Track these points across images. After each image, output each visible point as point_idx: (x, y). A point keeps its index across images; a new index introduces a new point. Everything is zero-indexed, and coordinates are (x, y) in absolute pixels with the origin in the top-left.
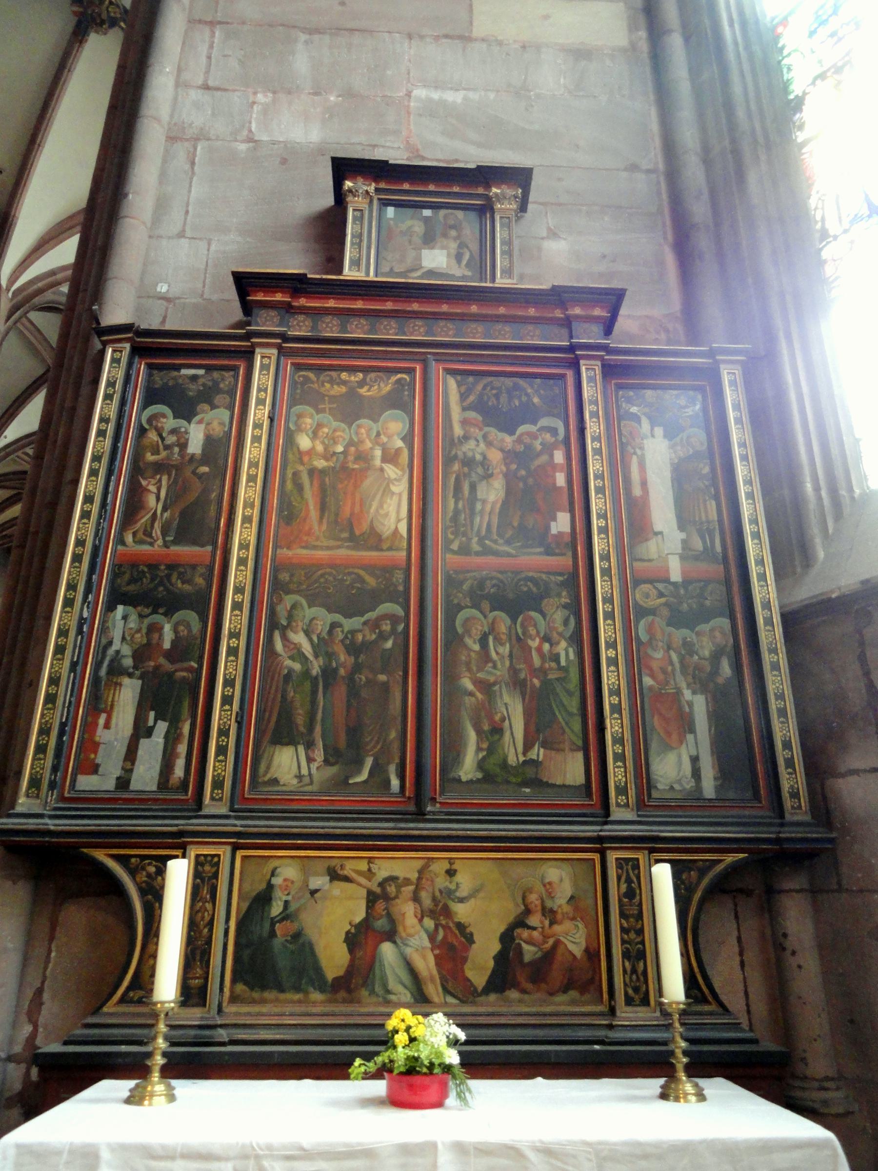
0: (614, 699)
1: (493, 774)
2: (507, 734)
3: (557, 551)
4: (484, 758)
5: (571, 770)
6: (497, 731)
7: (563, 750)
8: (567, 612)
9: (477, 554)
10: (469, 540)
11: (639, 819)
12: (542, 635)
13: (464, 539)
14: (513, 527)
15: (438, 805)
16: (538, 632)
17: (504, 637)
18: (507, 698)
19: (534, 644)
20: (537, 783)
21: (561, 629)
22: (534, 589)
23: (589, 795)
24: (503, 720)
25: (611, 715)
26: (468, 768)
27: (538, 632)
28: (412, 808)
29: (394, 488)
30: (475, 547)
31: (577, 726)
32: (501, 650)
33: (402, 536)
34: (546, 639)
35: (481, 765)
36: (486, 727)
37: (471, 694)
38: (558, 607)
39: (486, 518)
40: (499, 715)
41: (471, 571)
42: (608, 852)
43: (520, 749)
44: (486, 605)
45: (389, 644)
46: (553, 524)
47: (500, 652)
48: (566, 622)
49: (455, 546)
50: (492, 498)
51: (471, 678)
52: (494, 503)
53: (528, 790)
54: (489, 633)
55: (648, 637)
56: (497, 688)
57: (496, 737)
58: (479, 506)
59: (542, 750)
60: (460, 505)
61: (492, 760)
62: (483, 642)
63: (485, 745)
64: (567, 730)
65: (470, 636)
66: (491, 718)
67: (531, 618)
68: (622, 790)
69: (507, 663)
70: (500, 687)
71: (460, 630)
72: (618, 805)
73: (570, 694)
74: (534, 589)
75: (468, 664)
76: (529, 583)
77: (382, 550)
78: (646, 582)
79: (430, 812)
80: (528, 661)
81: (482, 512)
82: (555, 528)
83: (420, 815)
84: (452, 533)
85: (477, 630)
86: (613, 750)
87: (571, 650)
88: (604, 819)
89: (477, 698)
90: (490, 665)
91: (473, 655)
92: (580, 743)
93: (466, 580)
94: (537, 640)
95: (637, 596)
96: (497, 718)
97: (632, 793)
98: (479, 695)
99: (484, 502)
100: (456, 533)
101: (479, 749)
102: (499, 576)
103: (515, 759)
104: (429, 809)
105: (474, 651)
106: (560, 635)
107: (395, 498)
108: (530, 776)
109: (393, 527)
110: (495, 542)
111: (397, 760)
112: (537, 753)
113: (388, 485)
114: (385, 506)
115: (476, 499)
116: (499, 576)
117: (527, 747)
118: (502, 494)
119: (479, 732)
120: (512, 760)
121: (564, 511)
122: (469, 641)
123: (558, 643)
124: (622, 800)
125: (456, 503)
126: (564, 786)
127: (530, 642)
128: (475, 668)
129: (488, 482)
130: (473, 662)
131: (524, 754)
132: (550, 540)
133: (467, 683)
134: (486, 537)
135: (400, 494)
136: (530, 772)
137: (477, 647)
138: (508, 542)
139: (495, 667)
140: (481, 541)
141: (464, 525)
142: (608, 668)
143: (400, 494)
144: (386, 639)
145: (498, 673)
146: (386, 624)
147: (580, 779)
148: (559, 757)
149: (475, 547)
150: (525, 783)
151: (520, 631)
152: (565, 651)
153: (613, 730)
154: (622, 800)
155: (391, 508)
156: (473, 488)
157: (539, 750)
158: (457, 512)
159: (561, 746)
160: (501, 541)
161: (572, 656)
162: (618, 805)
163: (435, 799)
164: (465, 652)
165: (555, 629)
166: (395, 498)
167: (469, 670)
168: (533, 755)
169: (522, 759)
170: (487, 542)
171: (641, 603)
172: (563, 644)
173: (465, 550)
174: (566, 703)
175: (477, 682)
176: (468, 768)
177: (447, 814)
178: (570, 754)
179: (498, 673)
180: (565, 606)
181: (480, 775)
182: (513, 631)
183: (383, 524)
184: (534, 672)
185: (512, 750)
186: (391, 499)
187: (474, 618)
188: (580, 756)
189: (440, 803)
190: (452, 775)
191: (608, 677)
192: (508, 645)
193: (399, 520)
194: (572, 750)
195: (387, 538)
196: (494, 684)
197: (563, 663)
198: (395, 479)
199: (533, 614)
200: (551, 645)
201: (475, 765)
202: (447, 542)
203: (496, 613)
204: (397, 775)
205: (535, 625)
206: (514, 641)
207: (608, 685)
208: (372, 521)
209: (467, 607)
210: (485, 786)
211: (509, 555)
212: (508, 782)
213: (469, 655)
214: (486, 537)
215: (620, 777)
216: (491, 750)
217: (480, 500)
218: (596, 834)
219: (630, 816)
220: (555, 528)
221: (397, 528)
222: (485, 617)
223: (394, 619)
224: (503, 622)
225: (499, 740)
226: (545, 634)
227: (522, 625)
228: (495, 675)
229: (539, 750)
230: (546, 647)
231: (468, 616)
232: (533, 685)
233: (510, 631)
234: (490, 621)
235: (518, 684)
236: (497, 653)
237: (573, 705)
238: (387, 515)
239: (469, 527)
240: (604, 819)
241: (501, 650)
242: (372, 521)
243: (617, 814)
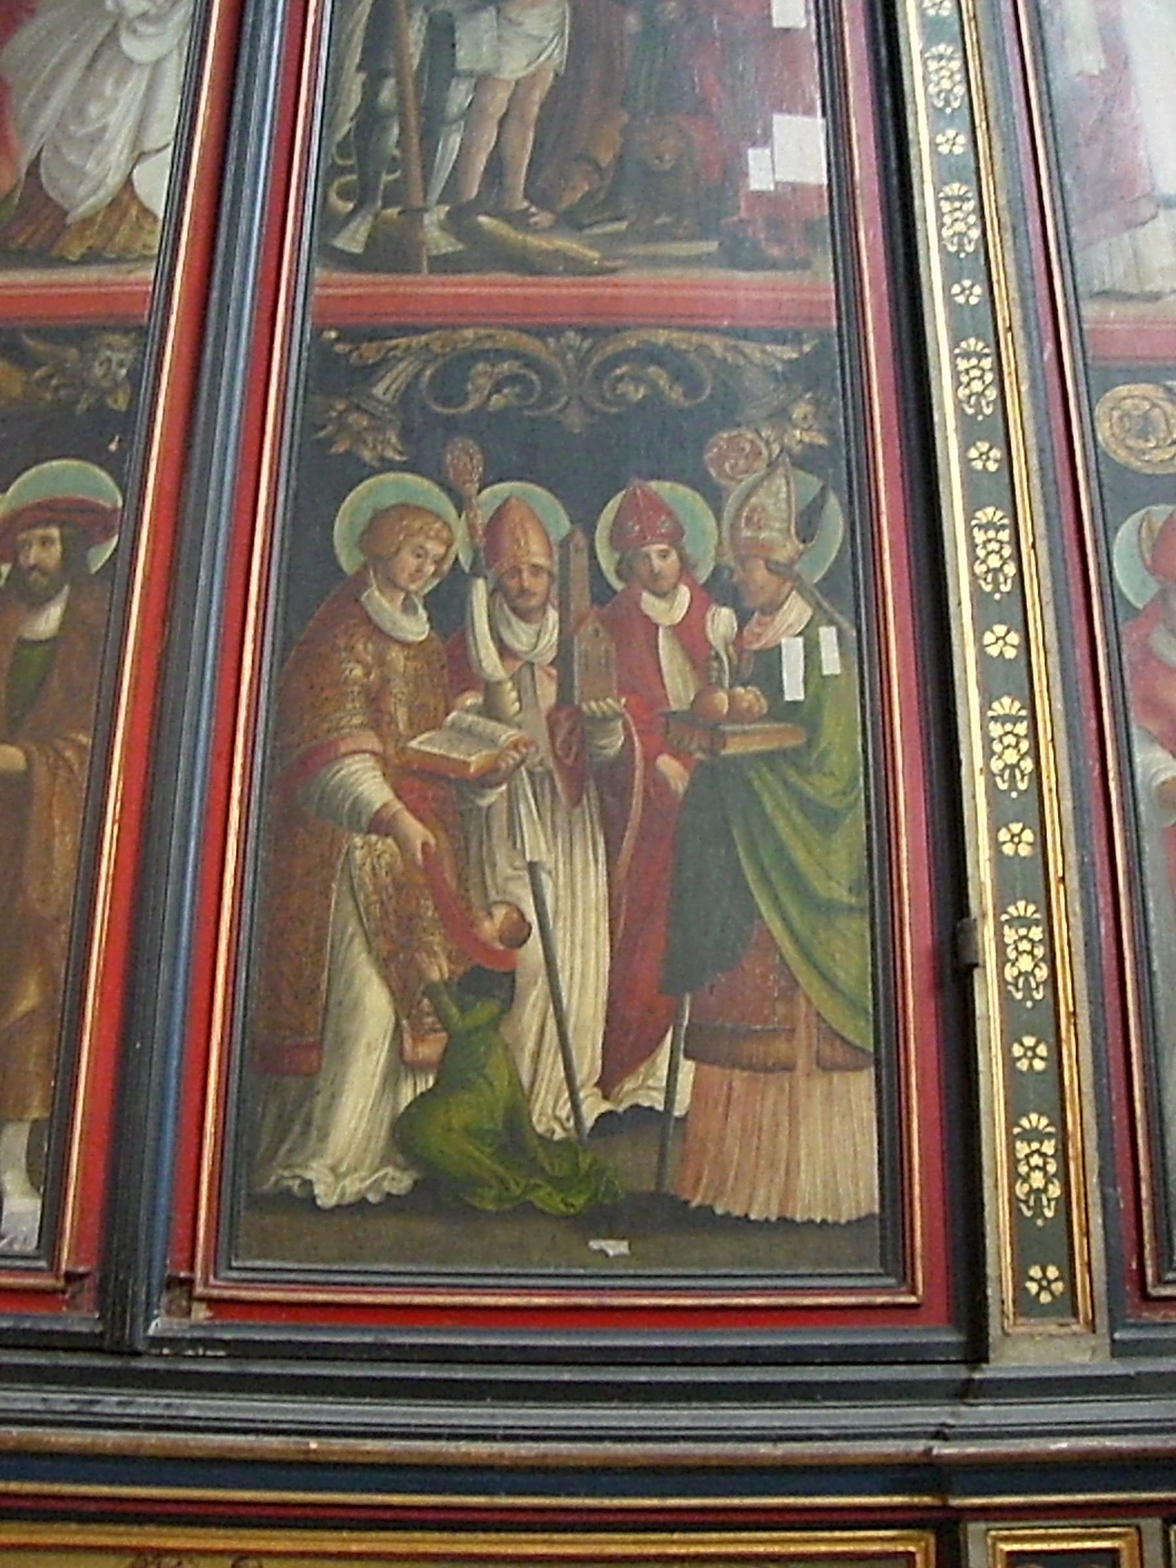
0: (1015, 838)
1: (462, 1166)
2: (534, 998)
3: (775, 252)
4: (420, 1101)
5: (823, 1151)
6: (489, 982)
7: (789, 1067)
8: (813, 484)
9: (444, 264)
10: (413, 215)
11: (1118, 1368)
12: (703, 575)
13: (392, 212)
14: (598, 168)
15: (201, 1313)
16: (686, 568)
17: (538, 585)
18: (536, 842)
19: (669, 610)
20: (664, 1215)
21: (787, 549)
22: (676, 395)
23: (898, 1264)
24: (517, 935)
25: (1000, 909)
26: (348, 1144)
27: (686, 568)
28: (81, 1320)
29: (129, 45)
30: (435, 234)
31: (851, 960)
32: (520, 636)
33: (146, 212)
34: (719, 589)
35: (404, 1135)
36: (438, 969)
37: (381, 825)
38: (772, 465)
39: (489, 138)
40: (500, 913)
41: (417, 331)
42: (975, 1528)
43: (589, 1062)
44: (464, 457)
45: (49, 621)
46: (756, 158)
47: (520, 646)
48: (808, 525)
49: (352, 240)
50: (515, 66)
51: (381, 758)
52: (521, 87)
53: (616, 1248)
54: (475, 573)
55: (1153, 588)
56: (493, 797)
57: (484, 1011)
58: (459, 96)
59: (687, 1068)
60: (387, 94)
61: (462, 1112)
62: (447, 606)
63: (430, 1050)
64: (804, 975)
65: (390, 584)
66: (459, 925)
67: (658, 506)
68: (1044, 1240)
69: (548, 693)
70: (512, 798)
71: (348, 559)
72: (1025, 1305)
73: (825, 820)
74: (676, 395)
75: (374, 700)
76: (652, 369)
77: (63, 262)
78: (1132, 377)
79: (158, 1342)
80: (642, 684)
81: (472, 115)
82: (762, 172)
83: (112, 1355)
84: (344, 194)
85: (419, 562)
86: (1010, 1062)
87: (827, 635)
88: (962, 1373)
89: (403, 843)
90: (471, 699)
91: (396, 656)
92: (861, 1033)
93: (384, 363)
94: (684, 594)
95: (1104, 432)
96: (490, 928)
97: (1091, 1247)
98: (416, 831)
99: (482, 81)
100: (362, 196)
101: (400, 1064)
102: (532, 345)
103: (565, 1110)
104: (154, 1328)
105: (405, 645)
106: (783, 572)
107: (137, 83)
108: (628, 1183)
109: (114, 180)
110: (519, 220)
111: (36, 1111)
112: (667, 1080)
113: (112, 36)
114: (93, 110)
115: (454, 74)
116: (532, 345)
117: (623, 1052)
118: (556, 54)
119: (405, 994)
120: (549, 1113)
121: (808, 111)
122: (382, 604)
123: (773, 607)
124: (1045, 1284)
125: (371, 91)
126: (785, 1223)
127: (650, 604)
128: (402, 715)
129: (499, 11)
130: (398, 687)
131: (606, 1085)
132: (743, 214)
133: (369, 784)
134: (476, 206)
135: (157, 65)
136: (631, 1166)
137: (417, 628)
138: (571, 221)
139: (491, 710)
140: (459, 220)
141: (393, 164)
142: (986, 705)
143: (157, 65)
144: (39, 602)
145: (507, 735)
146: (45, 542)
147: (857, 1191)
148: (772, 1097)
149: (435, 234)
150: (602, 1218)
151: (607, 561)
152: (807, 648)
153: (1010, 973)
154: (1045, 1284)
155: (113, 118)
156: (442, 36)
157: (673, 1069)
158: (370, 118)
159: (781, 1047)
160: (543, 218)
161: (831, 662)
162: (1025, 1305)
163: (190, 1282)
164: (365, 649)
165: (763, 549)
166: (137, 83)
167: (378, 721)
168: (645, 1089)
169: (593, 1107)
170: (483, 219)
171: (1121, 455)
172: (796, 610)
173: (391, 252)
174: (800, 855)
175: (415, 779)
176: (348, 1144)
177: (240, 1350)
178: (819, 1087)
179: (507, 735)
180: (806, 460)
181: (400, 1182)
182: (579, 562)
183: (80, 175)
184: (659, 725)
185: (552, 1069)
186: (119, 83)
187: (405, 509)
188: (861, 1088)
189: (211, 1302)
190: (277, 1177)
191: (988, 740)
192: (553, 615)
193: (139, 156)
194: (825, 1066)
195: (87, 222)
196: (487, 779)
197: (794, 691)
198: (144, 16)
199: (663, 488)
200: (743, 618)
201: (384, 1132)
202: (328, 223)
203: (503, 488)
204: (31, 1170)
205: (675, 538)
206: (581, 600)
207: (990, 776)
208: (35, 163)
209: (387, 466)
210: (429, 1229)
211: (575, 266)
212: (527, 1210)
213: (381, 661)
214: (476, 206)
215: (1037, 1180)
216: (452, 1075)
217: (470, 74)
218: (919, 1446)
219: (1079, 1353)
220: (762, 172)
221: (128, 182)
222: (461, 504)
223: (80, 520)
224: (540, 521)
225: (495, 1024)
226: (716, 573)
227: (617, 538)
228: (493, 742)
229: (673, 1069)
230: (721, 622)
231: (390, 500)
232: (656, 781)
233: (564, 563)
234: (482, 518)
235: (588, 778)
236: (504, 651)
237: (836, 868)
238: (95, 139)
239: (416, 171)
240: (962, 1373)
241: (520, 636)
242: (35, 163)
243: (1024, 1348)
